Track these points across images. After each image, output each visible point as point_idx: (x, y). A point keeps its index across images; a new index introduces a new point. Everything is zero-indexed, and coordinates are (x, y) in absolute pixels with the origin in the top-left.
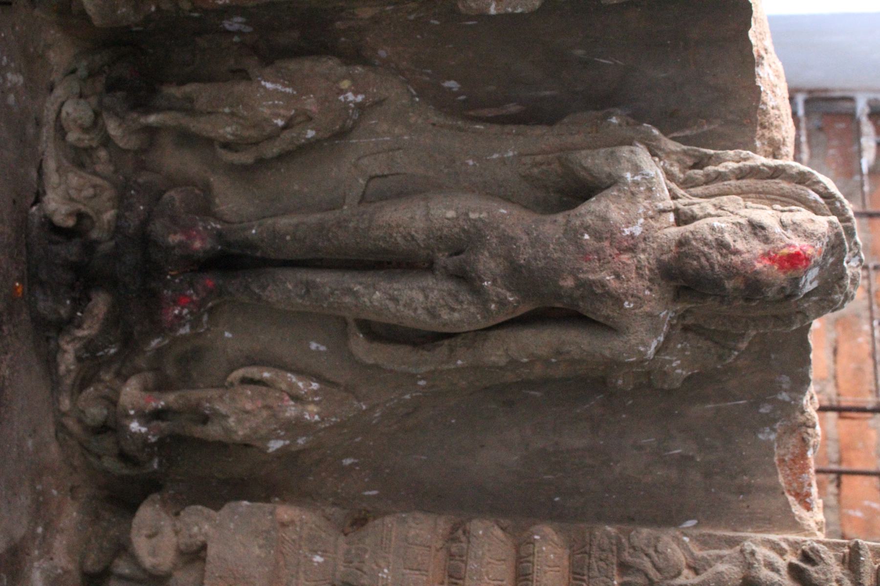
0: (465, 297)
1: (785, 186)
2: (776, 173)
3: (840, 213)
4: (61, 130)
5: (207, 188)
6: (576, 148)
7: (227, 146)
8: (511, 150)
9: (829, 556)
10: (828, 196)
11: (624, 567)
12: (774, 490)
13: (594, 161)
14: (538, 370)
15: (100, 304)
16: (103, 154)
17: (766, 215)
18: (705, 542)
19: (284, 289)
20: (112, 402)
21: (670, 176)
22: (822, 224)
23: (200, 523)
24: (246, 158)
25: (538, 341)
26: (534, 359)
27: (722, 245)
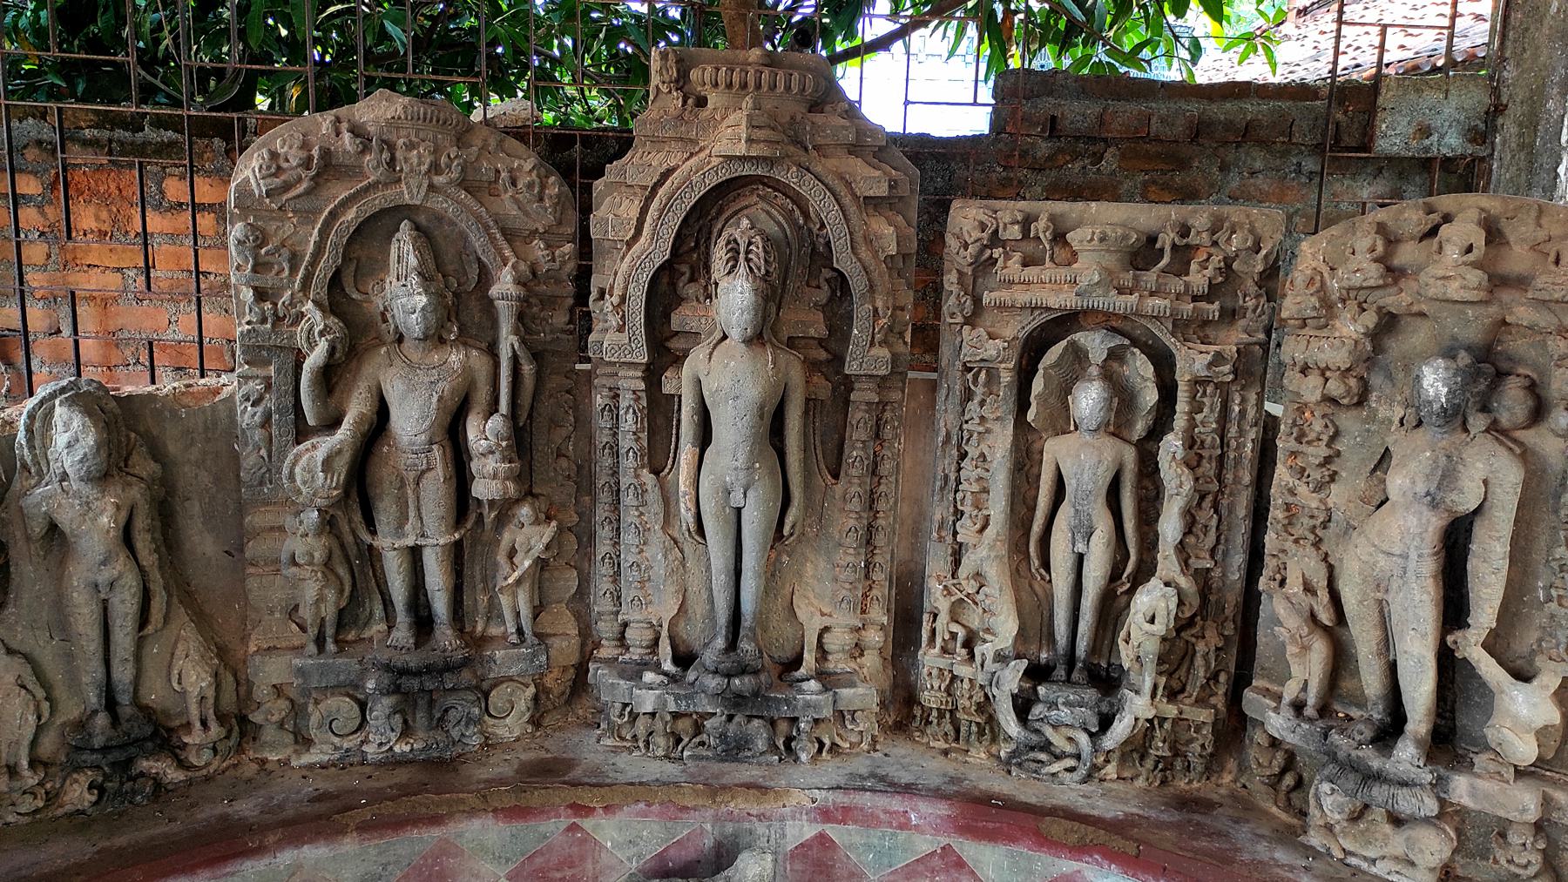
0: (122, 582)
1: (37, 424)
2: (29, 430)
3: (53, 396)
4: (37, 811)
5: (64, 725)
6: (28, 539)
7: (39, 718)
8: (27, 570)
9: (245, 390)
10: (42, 403)
11: (261, 483)
12: (214, 407)
13: (38, 529)
14: (158, 535)
15: (144, 764)
16: (48, 786)
17: (61, 439)
18: (246, 444)
19: (123, 674)
20: (200, 747)
21: (38, 484)
22: (60, 412)
23: (262, 692)
24: (46, 706)
25: (143, 542)
26: (154, 540)
27: (81, 461)
